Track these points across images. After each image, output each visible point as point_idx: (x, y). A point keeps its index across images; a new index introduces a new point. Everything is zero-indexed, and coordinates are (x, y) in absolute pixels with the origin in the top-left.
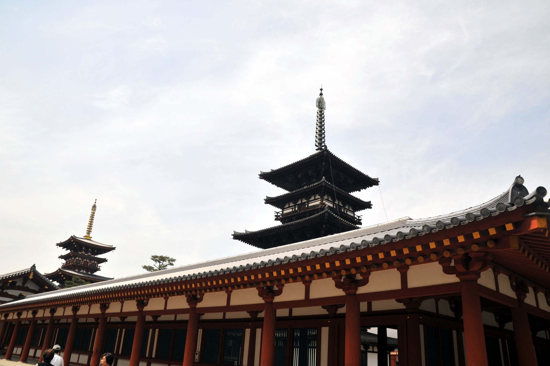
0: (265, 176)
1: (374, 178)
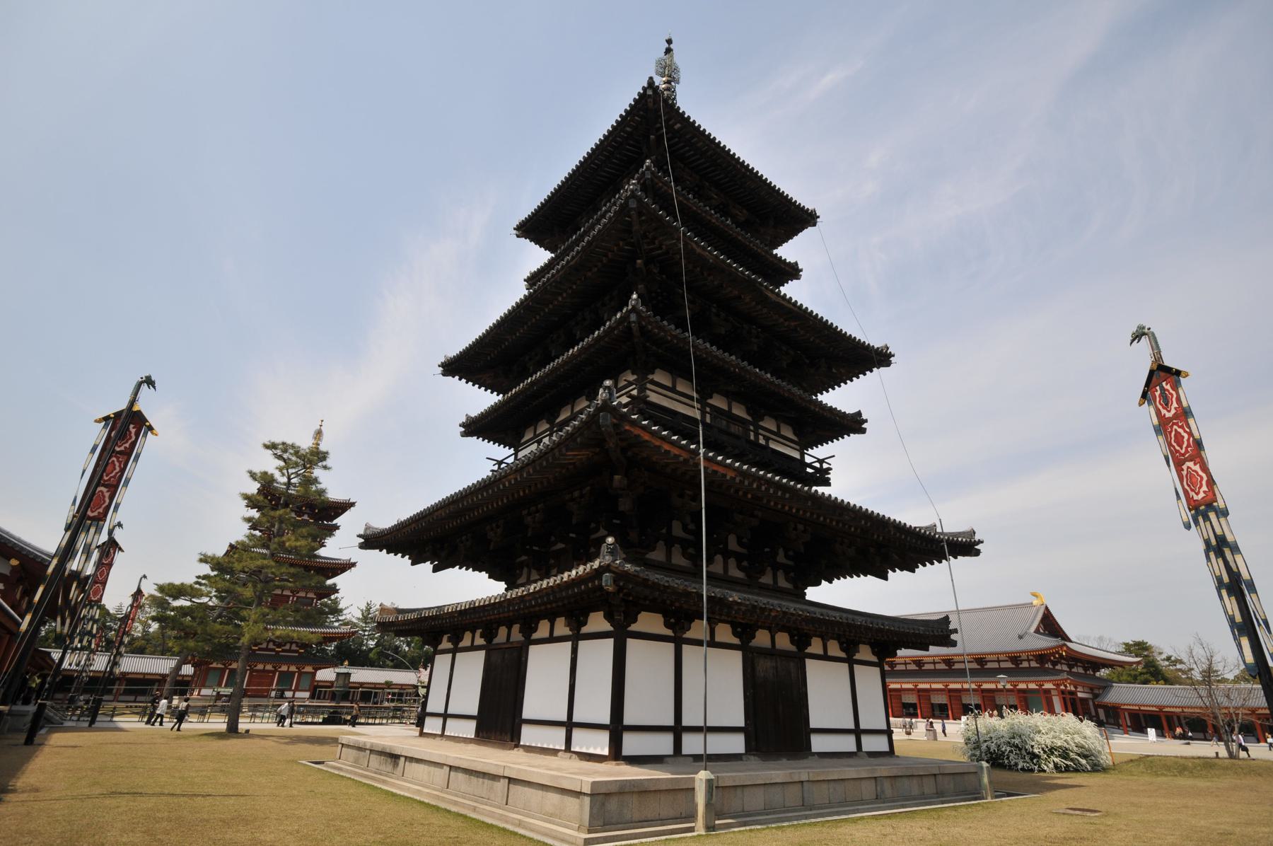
0: (453, 367)
1: (879, 346)
